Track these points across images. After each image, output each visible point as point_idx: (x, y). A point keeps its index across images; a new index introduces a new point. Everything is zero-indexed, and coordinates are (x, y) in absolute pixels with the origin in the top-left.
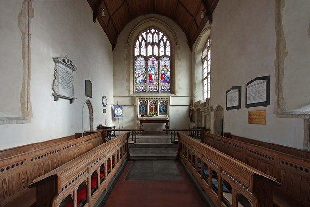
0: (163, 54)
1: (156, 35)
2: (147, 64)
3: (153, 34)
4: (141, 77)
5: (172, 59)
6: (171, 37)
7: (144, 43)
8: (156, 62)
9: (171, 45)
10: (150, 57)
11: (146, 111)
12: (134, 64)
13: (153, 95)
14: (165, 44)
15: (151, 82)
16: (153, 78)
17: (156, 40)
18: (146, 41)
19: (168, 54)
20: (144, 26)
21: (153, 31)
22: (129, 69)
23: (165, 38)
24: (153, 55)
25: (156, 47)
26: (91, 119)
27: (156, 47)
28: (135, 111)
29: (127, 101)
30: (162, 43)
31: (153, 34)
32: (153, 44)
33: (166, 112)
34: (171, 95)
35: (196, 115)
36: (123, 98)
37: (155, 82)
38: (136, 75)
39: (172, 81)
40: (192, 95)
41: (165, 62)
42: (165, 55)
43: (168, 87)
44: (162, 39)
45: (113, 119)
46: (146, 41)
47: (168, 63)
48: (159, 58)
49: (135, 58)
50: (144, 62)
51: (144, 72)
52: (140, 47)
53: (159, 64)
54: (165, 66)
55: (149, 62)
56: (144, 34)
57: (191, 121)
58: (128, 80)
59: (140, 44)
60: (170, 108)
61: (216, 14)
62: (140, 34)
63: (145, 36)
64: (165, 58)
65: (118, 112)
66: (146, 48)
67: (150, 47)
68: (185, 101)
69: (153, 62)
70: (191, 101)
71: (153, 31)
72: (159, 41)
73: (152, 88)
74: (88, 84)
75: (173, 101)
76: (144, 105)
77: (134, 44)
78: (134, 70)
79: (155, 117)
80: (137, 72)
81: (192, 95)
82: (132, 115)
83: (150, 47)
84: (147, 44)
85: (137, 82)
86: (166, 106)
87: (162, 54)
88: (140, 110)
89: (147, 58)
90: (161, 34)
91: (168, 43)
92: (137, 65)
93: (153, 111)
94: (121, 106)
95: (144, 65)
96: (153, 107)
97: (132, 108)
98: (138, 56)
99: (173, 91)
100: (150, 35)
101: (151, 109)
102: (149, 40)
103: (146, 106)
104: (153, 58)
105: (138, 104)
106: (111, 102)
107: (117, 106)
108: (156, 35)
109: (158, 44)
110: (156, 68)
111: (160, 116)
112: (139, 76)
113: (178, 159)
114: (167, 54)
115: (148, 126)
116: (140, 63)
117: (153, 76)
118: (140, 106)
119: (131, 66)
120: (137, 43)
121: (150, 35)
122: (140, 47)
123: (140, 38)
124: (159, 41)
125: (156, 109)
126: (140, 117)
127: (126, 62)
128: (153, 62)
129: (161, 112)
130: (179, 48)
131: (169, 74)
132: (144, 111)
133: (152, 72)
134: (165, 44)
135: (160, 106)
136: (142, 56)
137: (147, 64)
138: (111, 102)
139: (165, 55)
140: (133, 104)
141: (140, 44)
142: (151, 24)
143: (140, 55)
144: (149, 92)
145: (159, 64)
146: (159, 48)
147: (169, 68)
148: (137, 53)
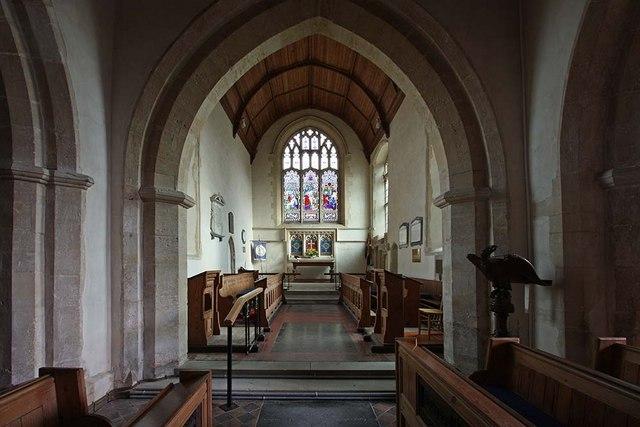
0: (326, 166)
1: (315, 139)
2: (301, 181)
3: (310, 137)
4: (294, 201)
5: (340, 173)
6: (339, 142)
7: (296, 150)
8: (316, 179)
9: (338, 152)
10: (307, 170)
11: (301, 249)
12: (282, 181)
13: (311, 226)
14: (329, 152)
15: (308, 207)
16: (311, 201)
17: (315, 146)
18: (300, 148)
19: (335, 166)
20: (298, 127)
21: (310, 132)
22: (275, 189)
23: (329, 143)
24: (311, 168)
25: (315, 155)
26: (233, 260)
27: (315, 155)
28: (285, 249)
29: (272, 235)
30: (324, 150)
31: (310, 137)
32: (310, 152)
33: (330, 251)
34: (338, 226)
35: (374, 255)
36: (263, 232)
37: (314, 208)
38: (286, 198)
39: (340, 206)
40: (369, 227)
41: (330, 178)
42: (329, 168)
43: (334, 214)
44: (324, 145)
45: (252, 259)
46: (300, 148)
47: (334, 179)
48: (320, 172)
49: (284, 172)
50: (297, 179)
51: (298, 193)
52: (292, 157)
53: (320, 181)
54: (330, 184)
55: (306, 179)
56: (297, 137)
57: (368, 263)
58: (274, 205)
59: (292, 152)
60: (336, 245)
61: (393, 126)
62: (291, 137)
63: (298, 141)
64: (329, 172)
65: (261, 251)
66: (301, 157)
67: (306, 155)
68: (360, 236)
69: (311, 179)
70: (369, 236)
71: (310, 132)
72: (321, 148)
73: (311, 216)
74: (231, 216)
75: (341, 235)
76: (298, 242)
77: (283, 152)
78: (283, 190)
79: (315, 259)
80: (286, 193)
81: (369, 227)
82: (280, 255)
83: (306, 155)
84: (301, 152)
85: (288, 207)
86: (331, 244)
87: (324, 166)
88: (292, 248)
89: (301, 173)
90: (323, 138)
91: (334, 150)
92: (286, 185)
93: (312, 250)
94: (264, 243)
95: (298, 182)
96: (311, 243)
97: (279, 247)
98: (289, 170)
99: (341, 221)
100: (306, 139)
101: (308, 247)
102: (305, 146)
103: (301, 243)
104: (311, 172)
105: (289, 239)
106: (250, 236)
107: (257, 243)
108: (315, 139)
109: (319, 152)
110: (316, 186)
111: (322, 258)
112: (290, 199)
113: (340, 303)
114: (332, 167)
115: (301, 270)
116: (291, 179)
117: (311, 199)
118: (293, 243)
119: (279, 184)
120: (287, 150)
121: (306, 139)
122: (292, 157)
123: (292, 143)
124: (321, 148)
125: (316, 247)
126: (292, 258)
127: (271, 179)
128: (311, 179)
129: (323, 250)
130: (349, 159)
131: (335, 195)
132: (298, 251)
133: (310, 193)
134: (329, 152)
135: (322, 243)
136: (295, 170)
137: (301, 181)
138: (250, 236)
139: (329, 168)
140: (282, 241)
141: (292, 152)
142: (308, 123)
143: (292, 168)
144: (305, 222)
145: (320, 181)
146: (320, 157)
147: (335, 187)
148: (286, 166)
